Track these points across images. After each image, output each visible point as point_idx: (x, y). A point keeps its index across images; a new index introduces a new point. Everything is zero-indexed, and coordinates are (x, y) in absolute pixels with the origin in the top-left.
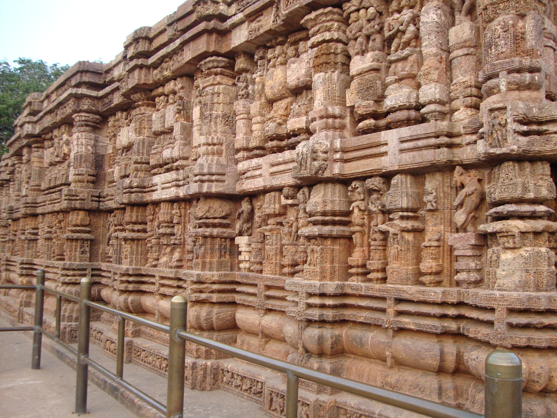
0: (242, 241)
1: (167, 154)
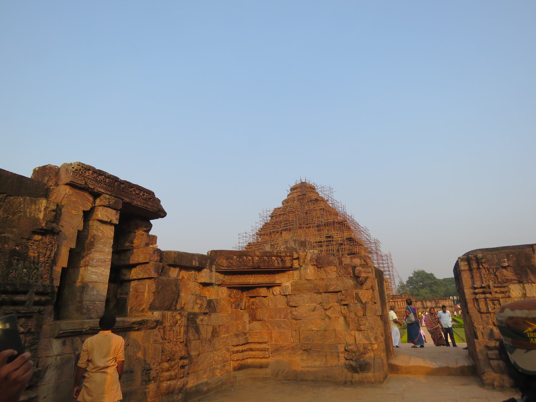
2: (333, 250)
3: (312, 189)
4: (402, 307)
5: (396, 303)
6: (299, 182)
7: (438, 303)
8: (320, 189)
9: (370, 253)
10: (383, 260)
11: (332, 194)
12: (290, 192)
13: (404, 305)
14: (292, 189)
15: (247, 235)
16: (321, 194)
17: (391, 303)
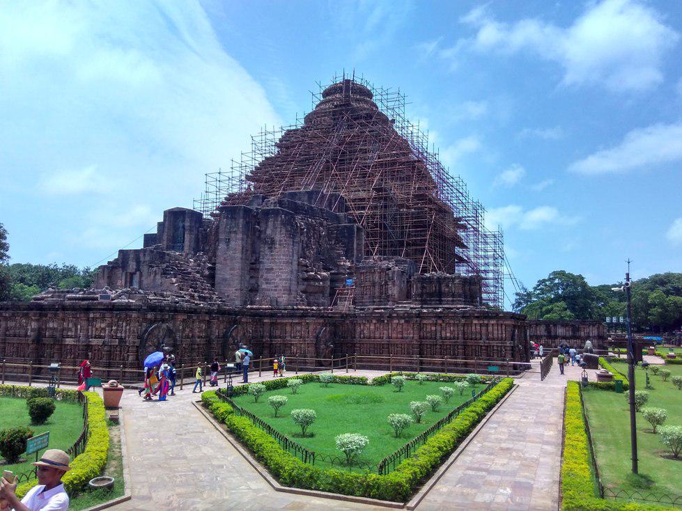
0: (90, 354)
1: (69, 333)
2: (385, 218)
3: (365, 93)
4: (496, 336)
5: (484, 328)
6: (340, 80)
7: (578, 330)
8: (379, 97)
9: (464, 227)
10: (486, 243)
11: (402, 108)
12: (322, 99)
13: (500, 332)
14: (326, 93)
15: (222, 178)
16: (381, 107)
17: (473, 328)
